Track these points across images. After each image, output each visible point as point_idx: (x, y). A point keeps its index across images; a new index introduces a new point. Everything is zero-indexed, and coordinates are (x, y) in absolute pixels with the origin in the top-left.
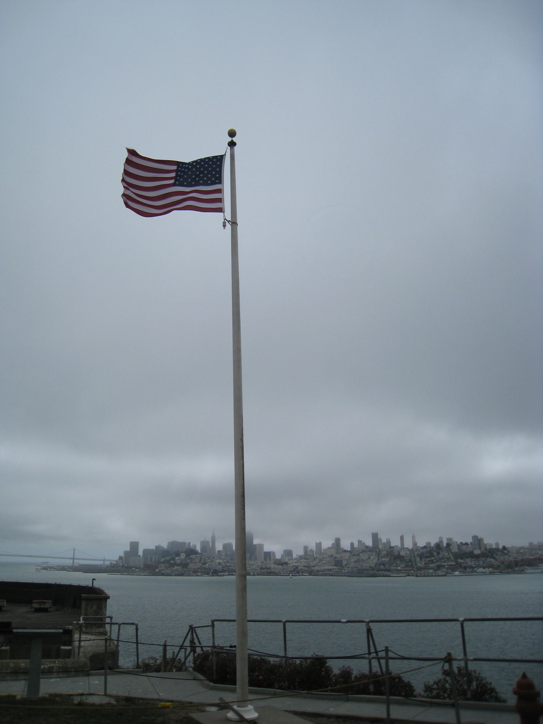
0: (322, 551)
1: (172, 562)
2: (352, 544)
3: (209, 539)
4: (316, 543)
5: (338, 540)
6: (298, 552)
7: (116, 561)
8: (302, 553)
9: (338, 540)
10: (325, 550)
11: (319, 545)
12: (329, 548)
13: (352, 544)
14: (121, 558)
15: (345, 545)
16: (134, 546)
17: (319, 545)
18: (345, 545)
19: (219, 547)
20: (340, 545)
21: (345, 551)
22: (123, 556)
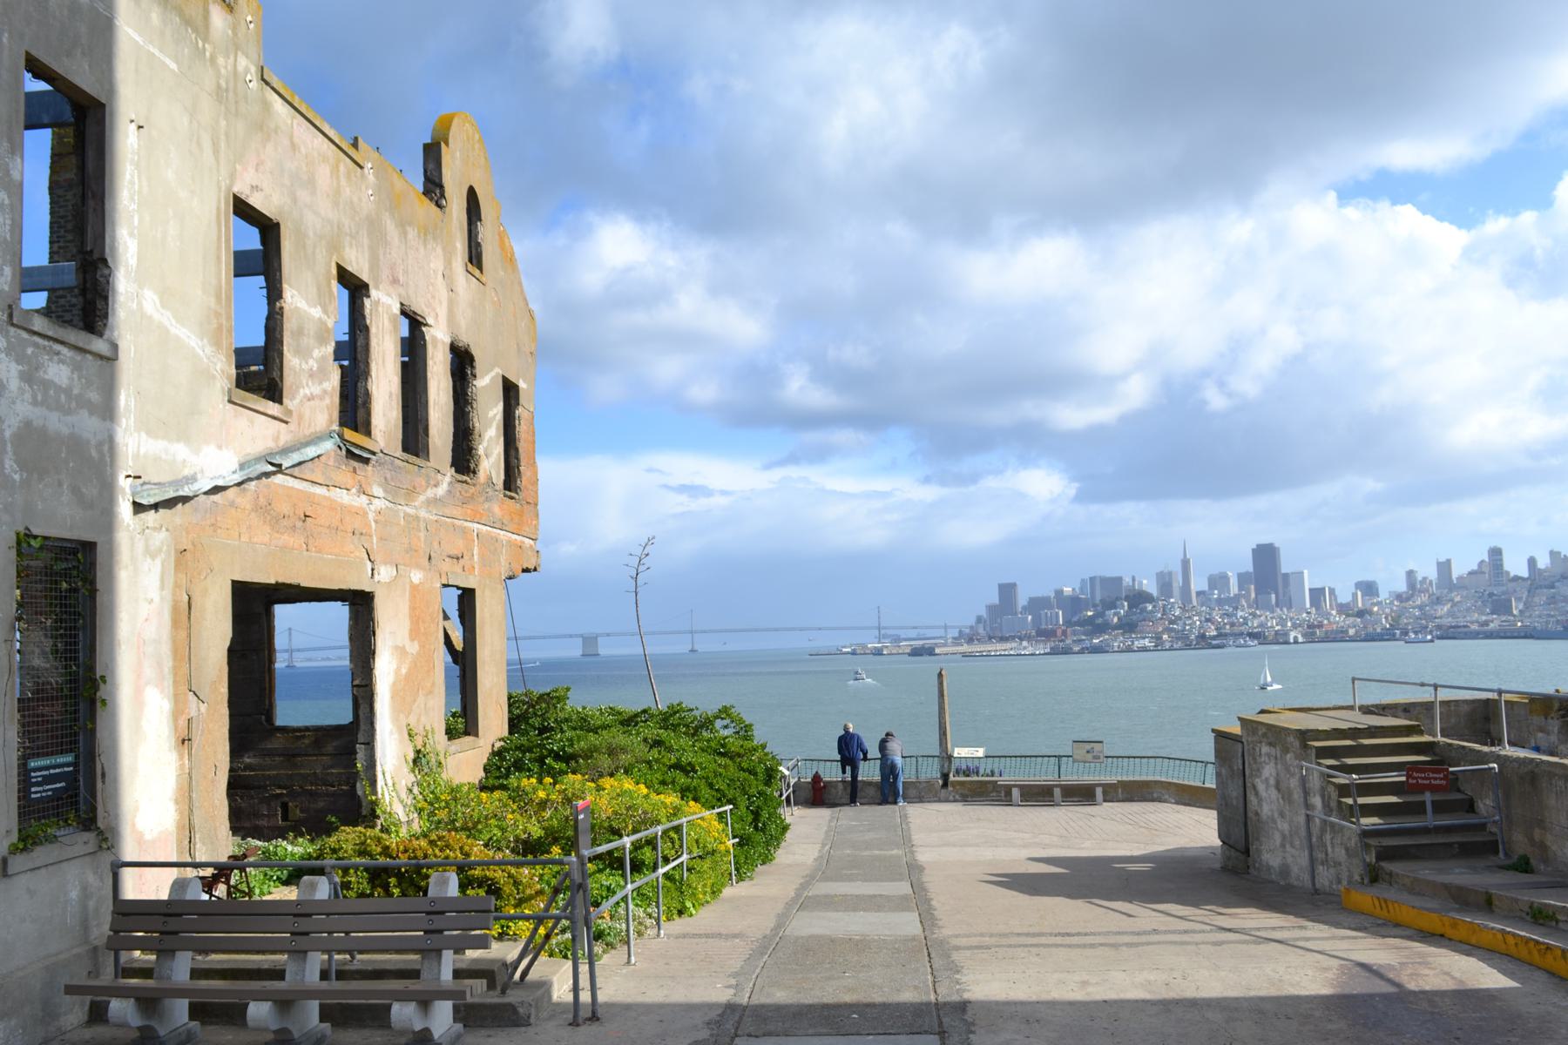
0: (1455, 582)
1: (1100, 621)
2: (1532, 562)
3: (1177, 568)
4: (1439, 564)
5: (1496, 553)
6: (1391, 582)
7: (971, 627)
8: (1402, 587)
9: (1496, 553)
10: (1460, 578)
11: (1444, 567)
12: (1470, 573)
13: (1532, 562)
14: (979, 619)
15: (1515, 565)
16: (1007, 591)
17: (1444, 567)
18: (1515, 565)
19: (1198, 583)
20: (1502, 565)
21: (1517, 579)
22: (985, 616)
